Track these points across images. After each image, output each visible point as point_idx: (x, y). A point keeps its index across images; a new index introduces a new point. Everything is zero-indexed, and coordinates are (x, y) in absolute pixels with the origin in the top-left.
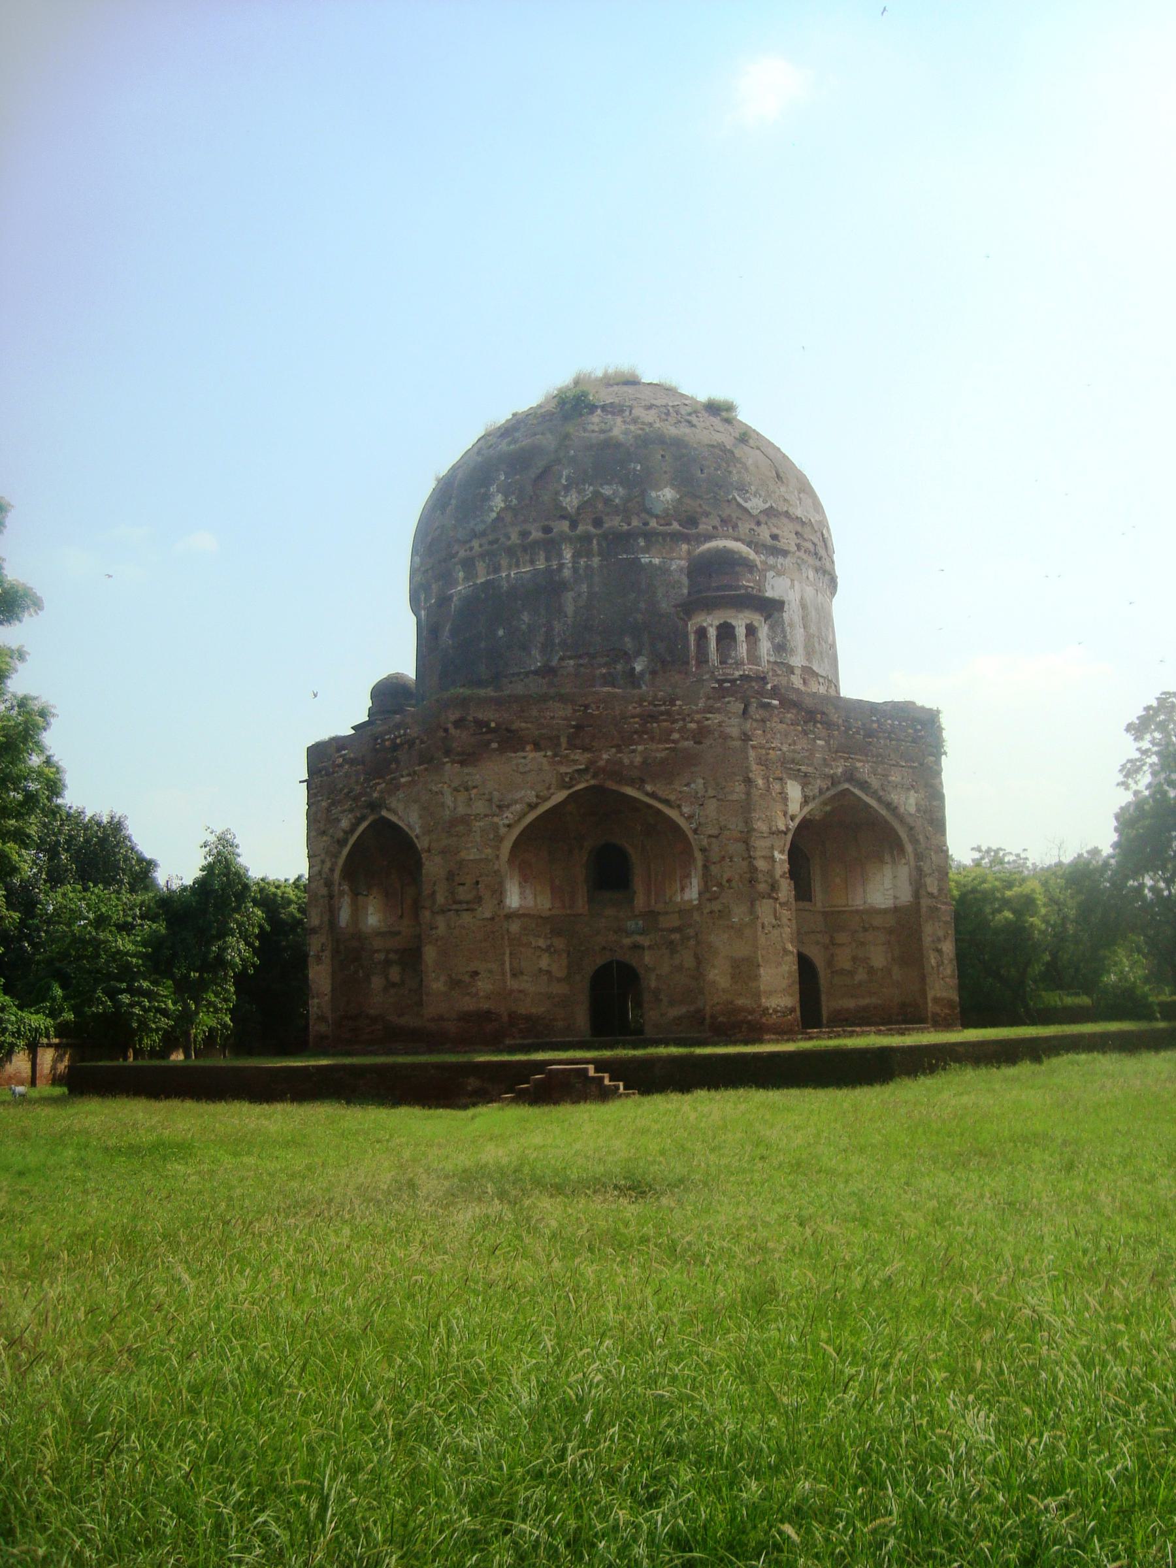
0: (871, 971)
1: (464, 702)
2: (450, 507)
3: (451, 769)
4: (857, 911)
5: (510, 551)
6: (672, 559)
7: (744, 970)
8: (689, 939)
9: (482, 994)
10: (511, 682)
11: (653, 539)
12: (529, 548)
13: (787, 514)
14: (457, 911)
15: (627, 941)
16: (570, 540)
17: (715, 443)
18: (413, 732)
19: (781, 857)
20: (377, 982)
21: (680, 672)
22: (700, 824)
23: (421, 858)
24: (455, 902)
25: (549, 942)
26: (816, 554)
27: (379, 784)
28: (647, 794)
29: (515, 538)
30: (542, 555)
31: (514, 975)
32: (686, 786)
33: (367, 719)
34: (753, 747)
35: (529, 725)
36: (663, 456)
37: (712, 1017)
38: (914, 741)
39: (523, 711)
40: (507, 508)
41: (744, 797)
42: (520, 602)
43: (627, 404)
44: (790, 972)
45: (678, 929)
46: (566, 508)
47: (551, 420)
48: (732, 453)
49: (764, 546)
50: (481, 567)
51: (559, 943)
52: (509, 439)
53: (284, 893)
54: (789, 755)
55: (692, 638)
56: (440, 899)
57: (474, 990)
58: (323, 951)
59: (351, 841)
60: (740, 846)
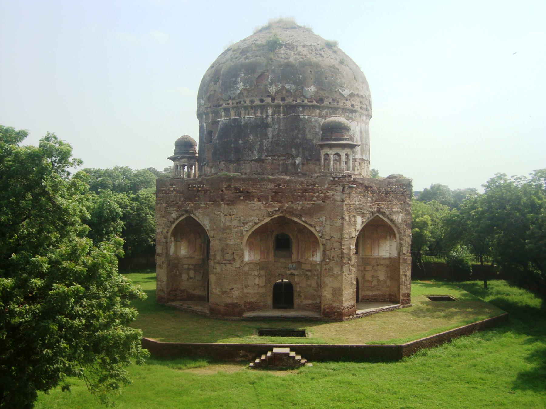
0: (379, 281)
1: (229, 179)
2: (218, 83)
3: (224, 207)
4: (375, 258)
5: (246, 108)
6: (312, 116)
7: (338, 292)
8: (314, 275)
9: (234, 297)
10: (244, 163)
11: (306, 108)
12: (255, 108)
13: (357, 95)
14: (225, 264)
15: (289, 272)
16: (272, 106)
17: (331, 65)
18: (207, 187)
19: (353, 247)
20: (184, 277)
21: (313, 164)
22: (323, 235)
23: (209, 239)
24: (224, 260)
25: (259, 273)
26: (367, 109)
27: (190, 204)
28: (302, 221)
29: (248, 103)
30: (259, 111)
31: (246, 287)
32: (319, 219)
33: (173, 154)
34: (346, 205)
35: (256, 191)
36: (311, 71)
37: (324, 310)
38: (402, 193)
39: (254, 185)
40: (244, 89)
41: (341, 225)
42: (249, 130)
43: (295, 44)
44: (353, 292)
45: (310, 271)
46: (270, 93)
47: (263, 50)
48: (338, 69)
49: (349, 110)
50: (232, 112)
51: (262, 272)
52: (244, 56)
53: (125, 202)
54: (358, 206)
55: (322, 158)
56: (218, 258)
57: (231, 295)
58: (163, 264)
59: (177, 222)
60: (339, 244)
